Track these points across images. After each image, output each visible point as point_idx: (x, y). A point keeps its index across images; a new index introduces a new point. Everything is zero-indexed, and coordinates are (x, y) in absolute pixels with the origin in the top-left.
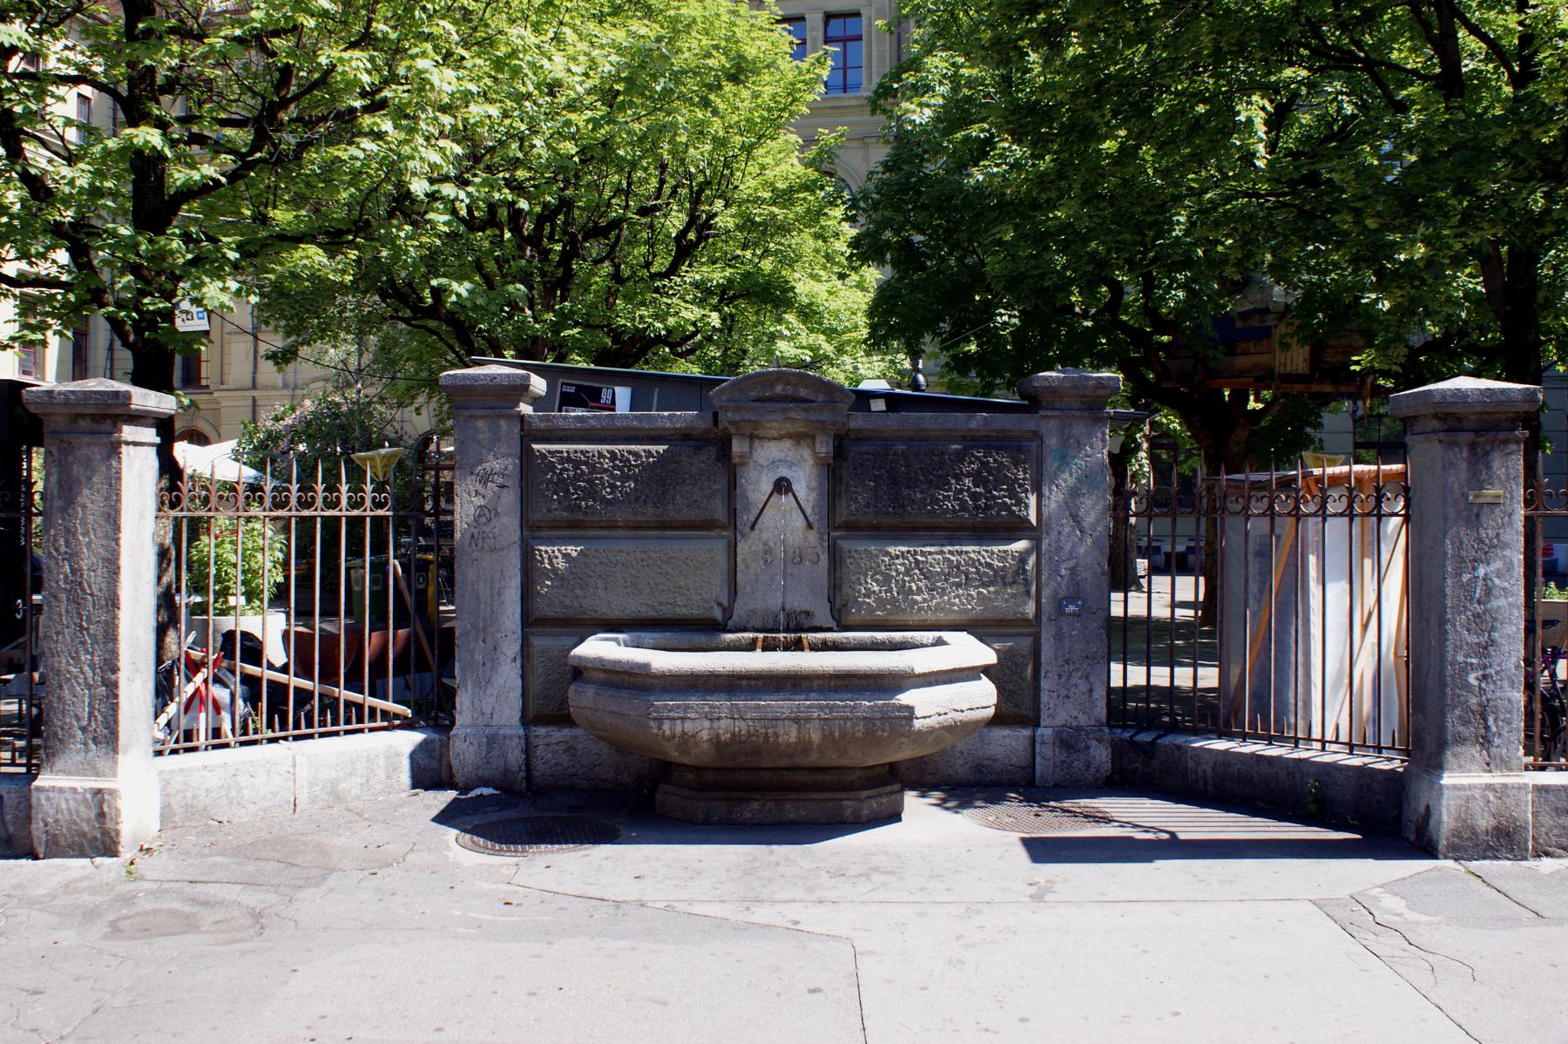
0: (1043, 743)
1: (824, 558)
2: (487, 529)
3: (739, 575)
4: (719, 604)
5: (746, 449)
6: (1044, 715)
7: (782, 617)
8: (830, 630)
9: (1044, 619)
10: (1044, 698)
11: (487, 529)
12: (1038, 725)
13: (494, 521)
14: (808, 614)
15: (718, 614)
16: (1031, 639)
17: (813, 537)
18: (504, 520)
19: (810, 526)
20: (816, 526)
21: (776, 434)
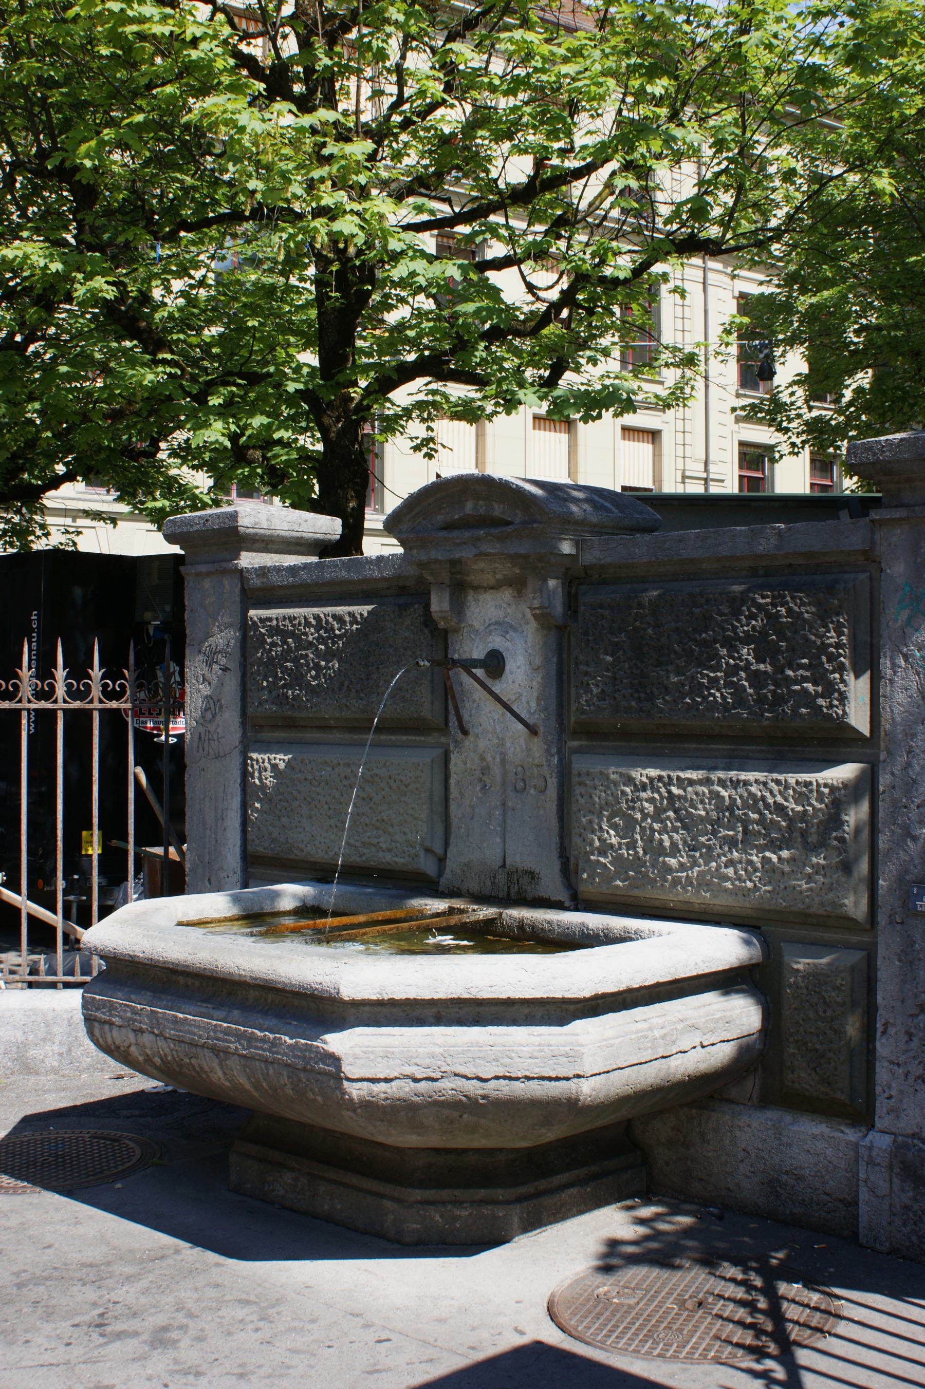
0: (871, 1162)
1: (553, 782)
2: (212, 728)
3: (453, 807)
4: (428, 850)
5: (446, 606)
6: (881, 1106)
7: (502, 879)
8: (559, 906)
9: (882, 919)
10: (882, 1074)
11: (212, 728)
12: (871, 1126)
13: (218, 717)
14: (532, 875)
15: (428, 866)
16: (862, 954)
17: (538, 746)
18: (227, 715)
19: (533, 730)
20: (541, 730)
21: (492, 582)
